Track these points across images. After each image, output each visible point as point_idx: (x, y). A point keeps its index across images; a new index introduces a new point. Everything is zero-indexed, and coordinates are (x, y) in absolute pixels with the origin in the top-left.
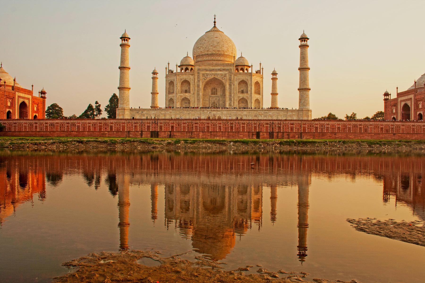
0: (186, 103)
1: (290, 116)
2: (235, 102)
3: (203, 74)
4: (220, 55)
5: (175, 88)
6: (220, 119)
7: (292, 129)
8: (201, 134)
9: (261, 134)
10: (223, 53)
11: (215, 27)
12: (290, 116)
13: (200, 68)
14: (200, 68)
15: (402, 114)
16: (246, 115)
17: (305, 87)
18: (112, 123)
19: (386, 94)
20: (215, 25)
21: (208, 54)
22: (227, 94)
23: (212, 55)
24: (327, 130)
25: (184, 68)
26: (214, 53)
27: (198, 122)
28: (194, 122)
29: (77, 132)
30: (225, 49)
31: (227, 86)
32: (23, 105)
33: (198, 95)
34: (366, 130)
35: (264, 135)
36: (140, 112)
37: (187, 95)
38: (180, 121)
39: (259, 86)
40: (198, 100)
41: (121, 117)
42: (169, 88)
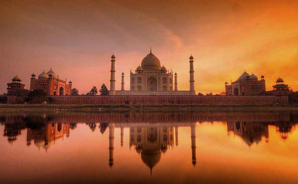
1: (186, 94)
6: (155, 95)
7: (188, 100)
8: (148, 102)
9: (174, 102)
12: (186, 94)
13: (146, 72)
15: (234, 92)
16: (166, 93)
18: (108, 97)
19: (226, 83)
21: (148, 66)
22: (158, 84)
23: (150, 66)
24: (203, 100)
26: (151, 64)
27: (147, 96)
28: (145, 96)
29: (91, 101)
31: (158, 80)
32: (61, 89)
33: (145, 84)
34: (220, 100)
35: (175, 102)
38: (138, 96)
40: (145, 87)
41: (112, 95)
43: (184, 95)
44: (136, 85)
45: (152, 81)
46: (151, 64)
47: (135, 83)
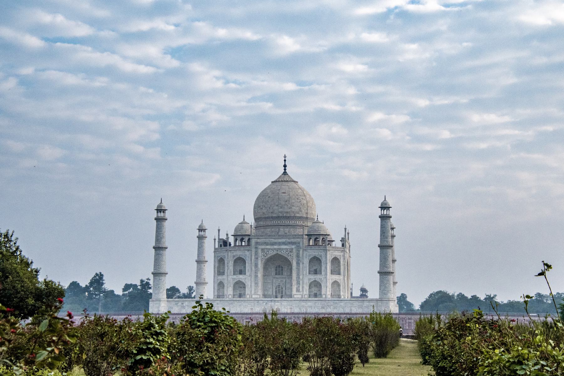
0: (241, 287)
2: (305, 286)
3: (262, 249)
4: (288, 218)
5: (226, 268)
10: (293, 215)
11: (285, 173)
13: (259, 241)
14: (259, 241)
17: (386, 270)
20: (285, 170)
23: (278, 218)
25: (239, 238)
26: (281, 215)
30: (295, 209)
33: (256, 276)
36: (180, 304)
37: (241, 277)
39: (339, 262)
40: (256, 284)
42: (219, 267)
43: (360, 311)
44: (230, 278)
45: (278, 266)
46: (281, 212)
47: (226, 274)
